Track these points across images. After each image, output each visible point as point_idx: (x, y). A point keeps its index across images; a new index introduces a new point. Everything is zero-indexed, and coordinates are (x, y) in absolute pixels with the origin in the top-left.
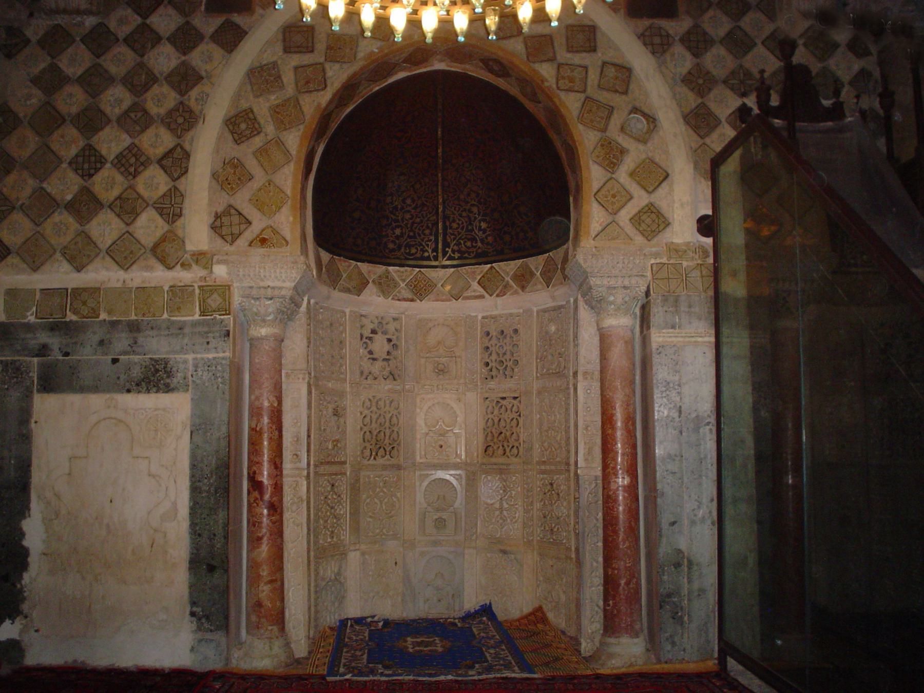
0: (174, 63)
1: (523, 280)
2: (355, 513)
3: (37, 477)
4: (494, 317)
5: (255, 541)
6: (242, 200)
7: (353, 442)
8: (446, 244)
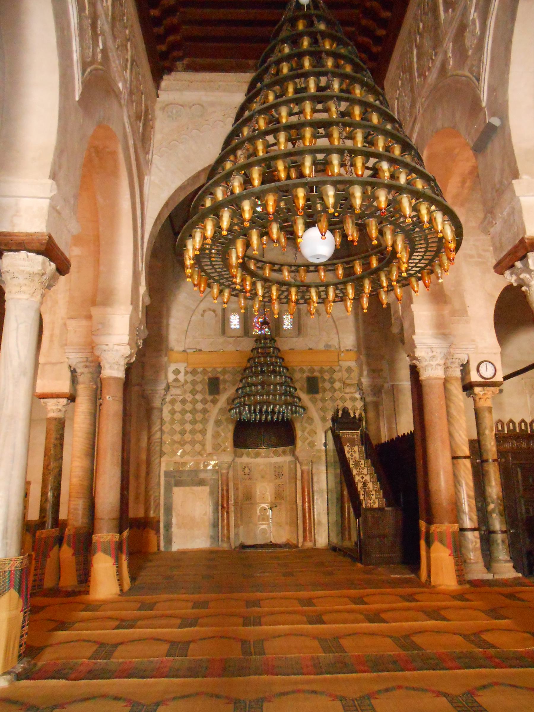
0: (202, 408)
1: (284, 453)
2: (241, 515)
3: (174, 506)
4: (277, 463)
5: (223, 520)
6: (220, 440)
8: (264, 443)
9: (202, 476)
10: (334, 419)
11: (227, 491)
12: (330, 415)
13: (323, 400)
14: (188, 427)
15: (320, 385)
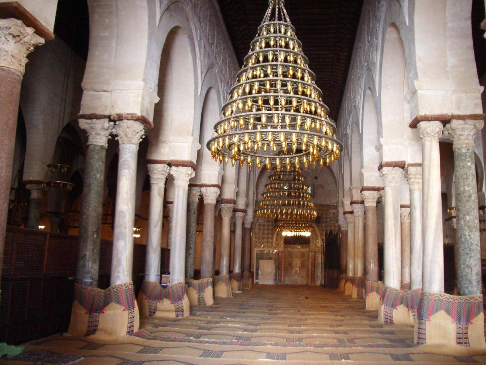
1: (306, 247)
7: (287, 264)
9: (271, 256)
10: (326, 234)
11: (281, 262)
12: (324, 233)
13: (322, 226)
14: (266, 236)
15: (321, 220)
